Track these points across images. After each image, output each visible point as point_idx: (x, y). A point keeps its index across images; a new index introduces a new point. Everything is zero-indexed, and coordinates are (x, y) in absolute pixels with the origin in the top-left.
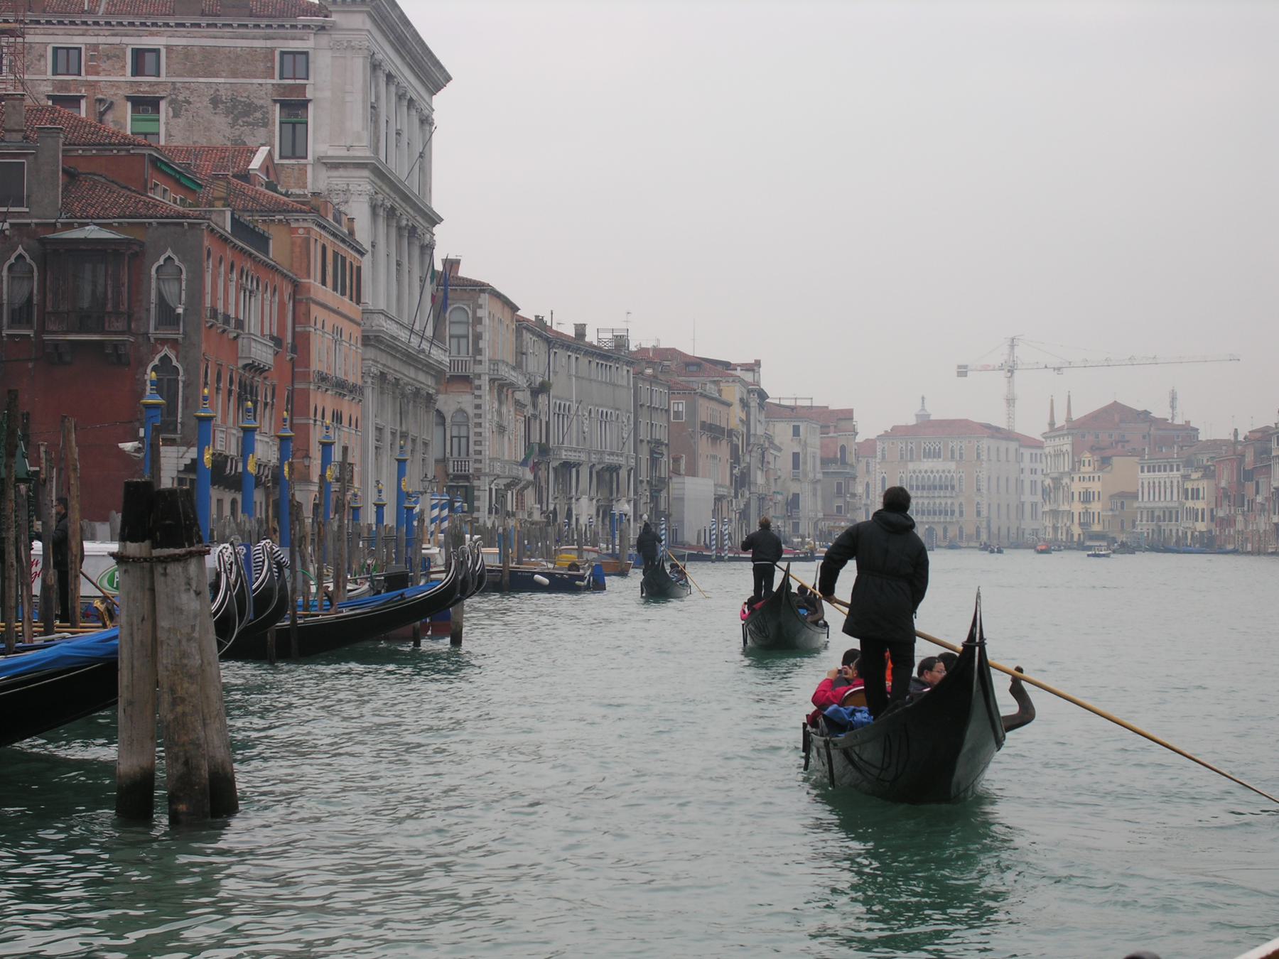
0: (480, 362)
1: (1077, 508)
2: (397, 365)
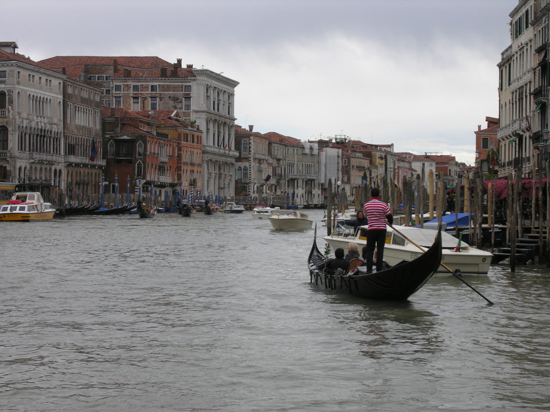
2: (217, 157)
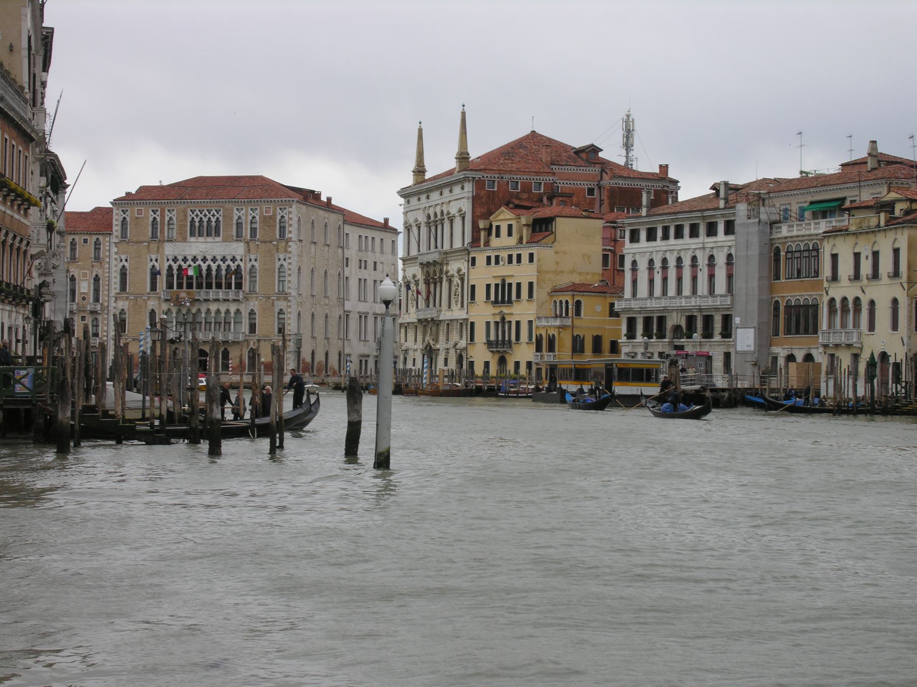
1: (483, 313)
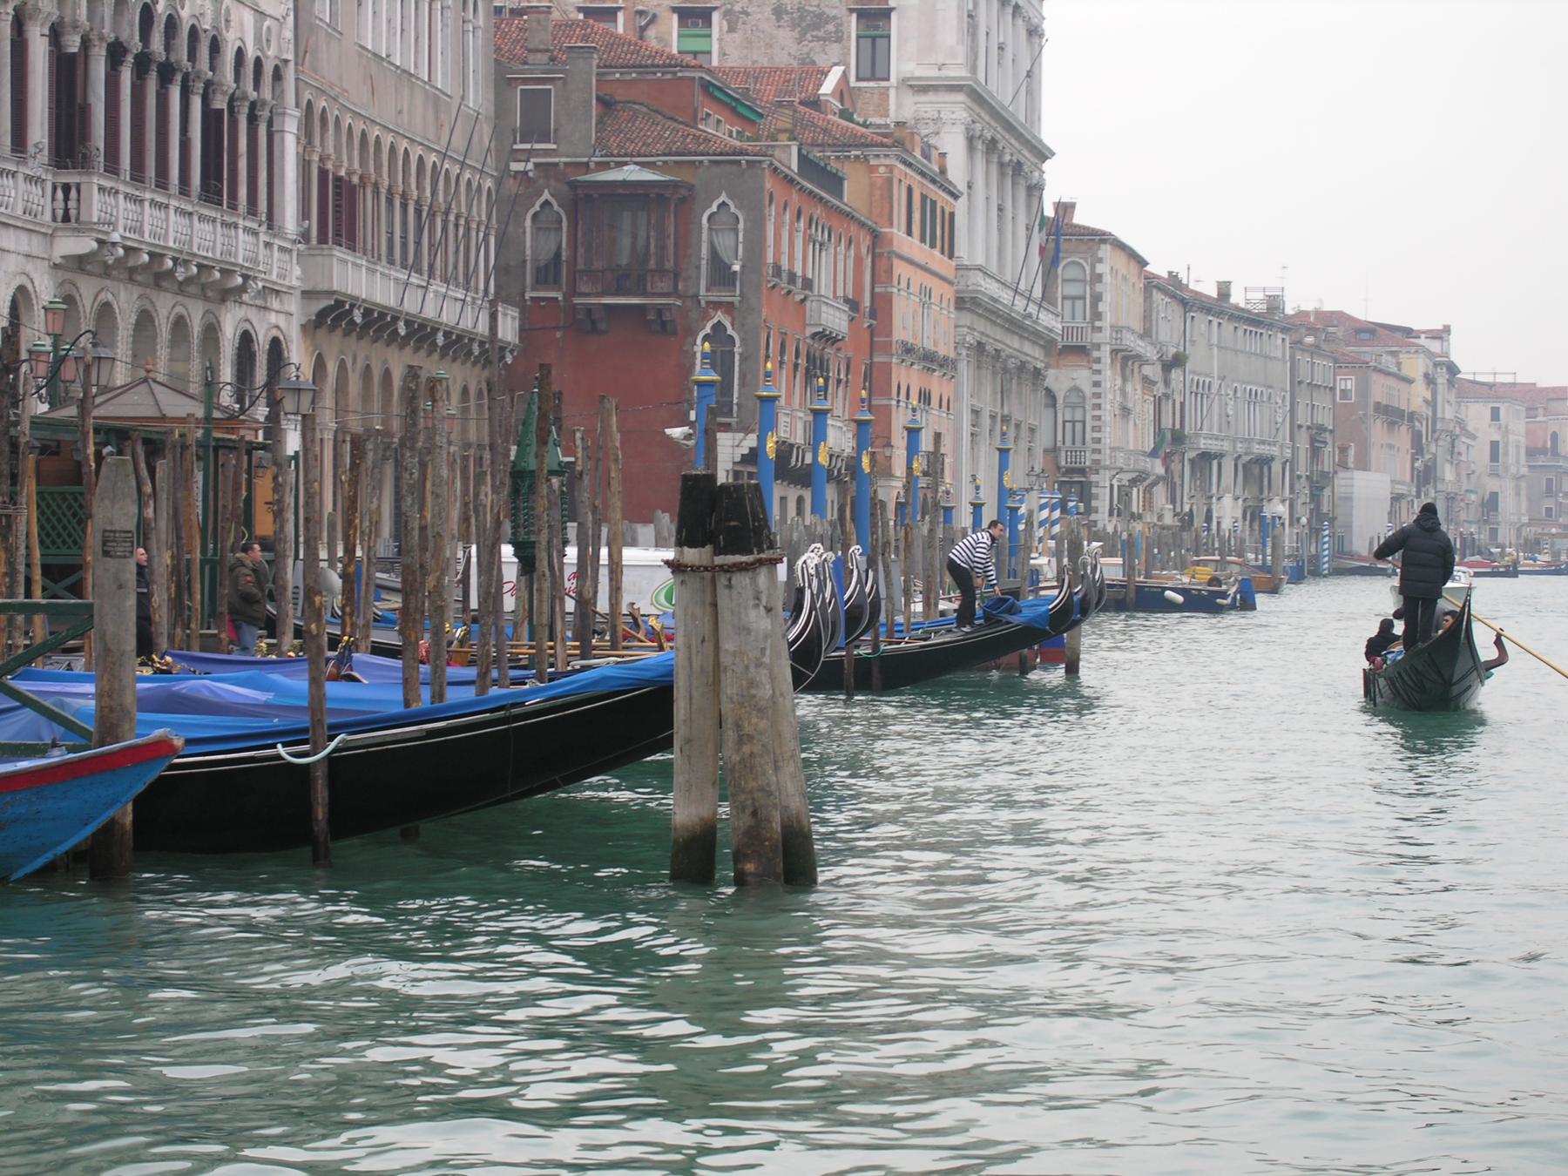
0: (1100, 329)
2: (998, 333)
